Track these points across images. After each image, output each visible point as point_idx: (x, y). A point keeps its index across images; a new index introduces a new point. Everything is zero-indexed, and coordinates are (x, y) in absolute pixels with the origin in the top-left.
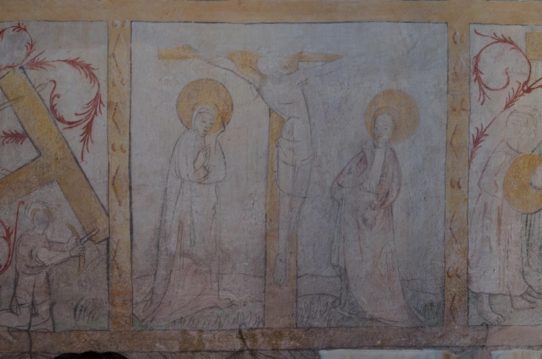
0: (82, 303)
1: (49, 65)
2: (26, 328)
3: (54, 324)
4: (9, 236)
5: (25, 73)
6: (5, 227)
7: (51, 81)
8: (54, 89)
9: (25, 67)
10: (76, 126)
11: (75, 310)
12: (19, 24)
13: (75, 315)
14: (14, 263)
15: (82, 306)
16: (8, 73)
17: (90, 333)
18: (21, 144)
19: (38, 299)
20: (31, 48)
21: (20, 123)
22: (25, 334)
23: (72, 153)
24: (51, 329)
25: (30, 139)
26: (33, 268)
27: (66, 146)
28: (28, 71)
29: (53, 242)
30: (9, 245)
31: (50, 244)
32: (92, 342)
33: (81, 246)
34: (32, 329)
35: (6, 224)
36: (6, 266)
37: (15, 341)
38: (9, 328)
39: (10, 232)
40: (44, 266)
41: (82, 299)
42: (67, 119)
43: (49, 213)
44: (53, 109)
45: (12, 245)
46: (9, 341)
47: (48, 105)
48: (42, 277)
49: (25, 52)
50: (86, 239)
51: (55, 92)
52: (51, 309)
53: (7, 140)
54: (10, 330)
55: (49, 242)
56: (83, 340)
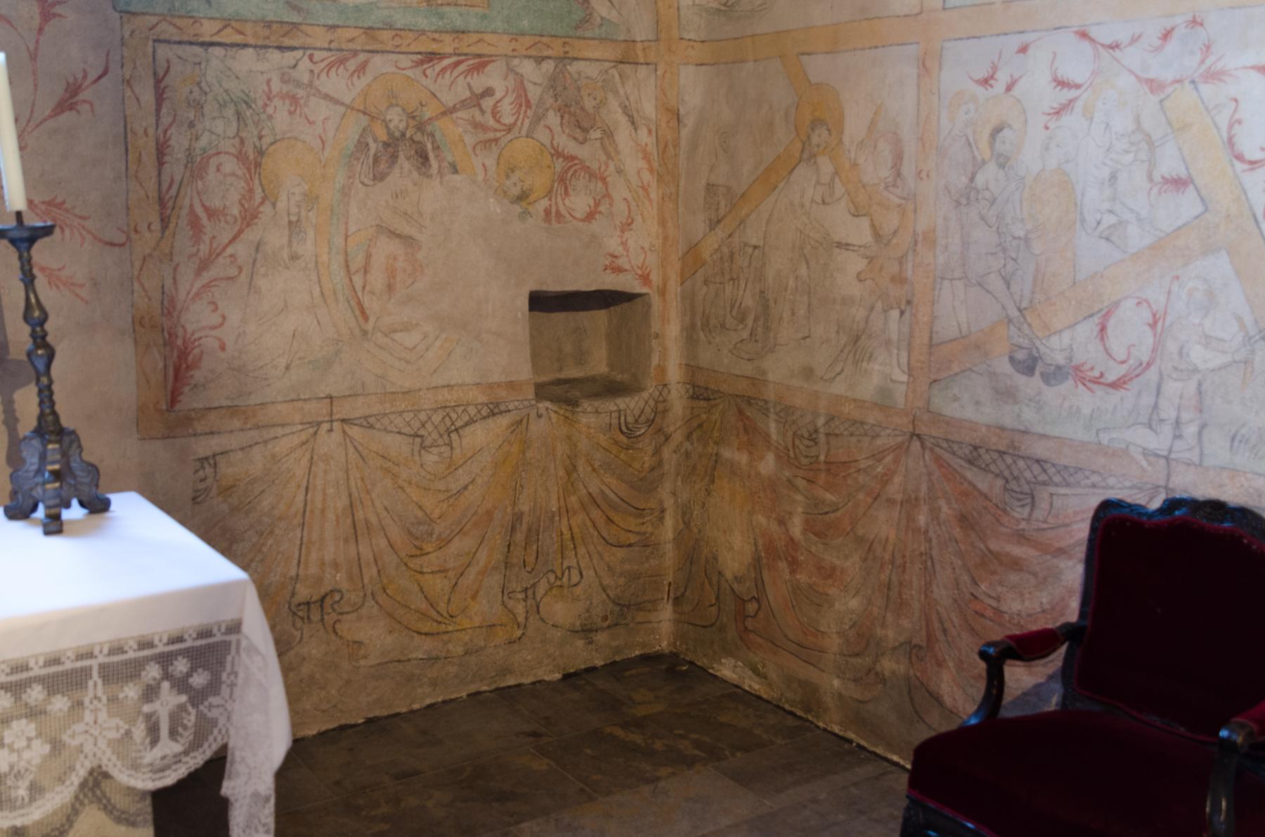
0: (1244, 431)
1: (1230, 76)
2: (1165, 453)
3: (1201, 454)
4: (1155, 323)
5: (1196, 89)
6: (1152, 310)
7: (1231, 99)
8: (1235, 111)
9: (1197, 80)
10: (1259, 167)
11: (1233, 439)
12: (1194, 17)
13: (1232, 446)
14: (1158, 361)
15: (1243, 436)
16: (1175, 90)
17: (1250, 476)
18: (1183, 193)
19: (1185, 416)
20: (1207, 51)
21: (1185, 162)
22: (1163, 461)
23: (1251, 209)
24: (1196, 460)
25: (1195, 186)
26: (1181, 371)
27: (1244, 197)
28: (1203, 88)
29: (1211, 337)
30: (1155, 335)
31: (1208, 341)
32: (1251, 491)
33: (1249, 348)
34: (1173, 456)
35: (1154, 307)
36: (1149, 365)
37: (1149, 468)
38: (1144, 449)
39: (1158, 316)
40: (1196, 370)
41: (1243, 425)
42: (1248, 157)
43: (1210, 294)
44: (1231, 142)
45: (1158, 338)
46: (1142, 467)
47: (1225, 135)
48: (1193, 385)
49: (1198, 57)
50: (1257, 337)
51: (1236, 117)
52: (1200, 433)
53: (1166, 187)
54: (1146, 453)
55: (1207, 337)
56: (1239, 485)
